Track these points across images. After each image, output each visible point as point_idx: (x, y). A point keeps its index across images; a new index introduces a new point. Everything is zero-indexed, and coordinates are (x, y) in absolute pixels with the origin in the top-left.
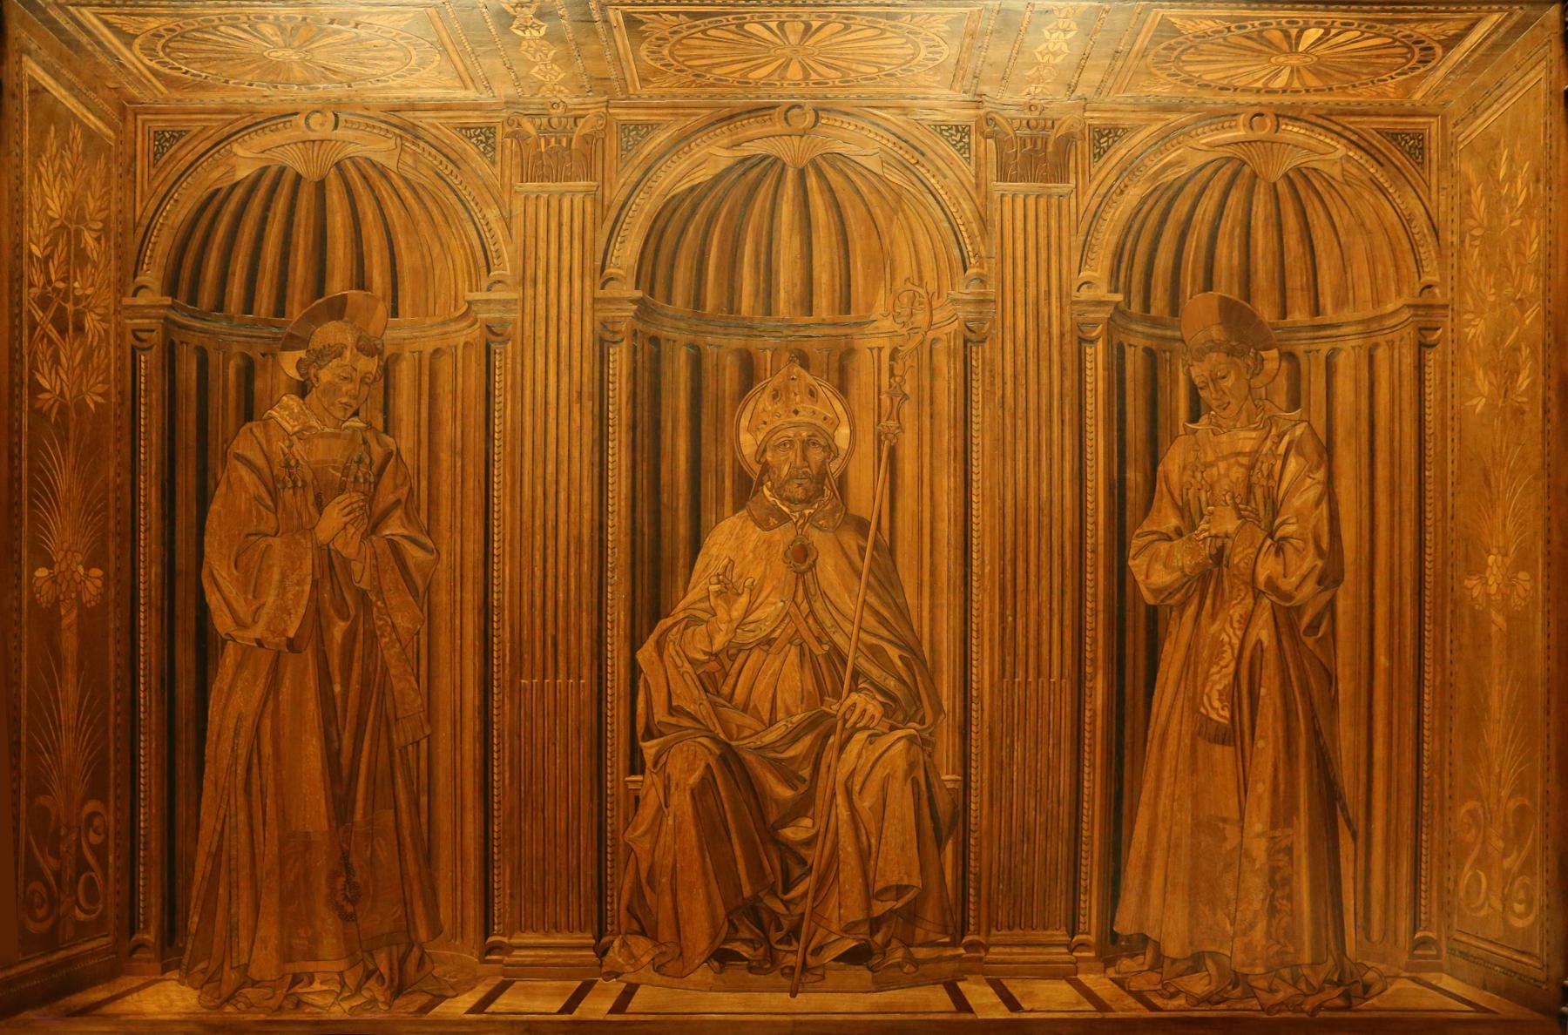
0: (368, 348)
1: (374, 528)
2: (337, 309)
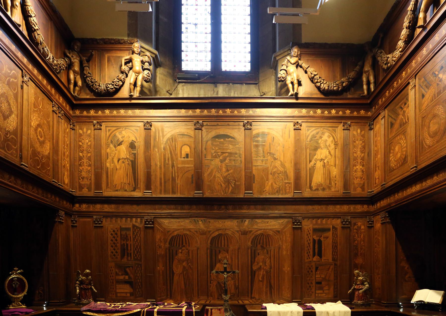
0: (187, 249)
1: (188, 264)
2: (184, 246)
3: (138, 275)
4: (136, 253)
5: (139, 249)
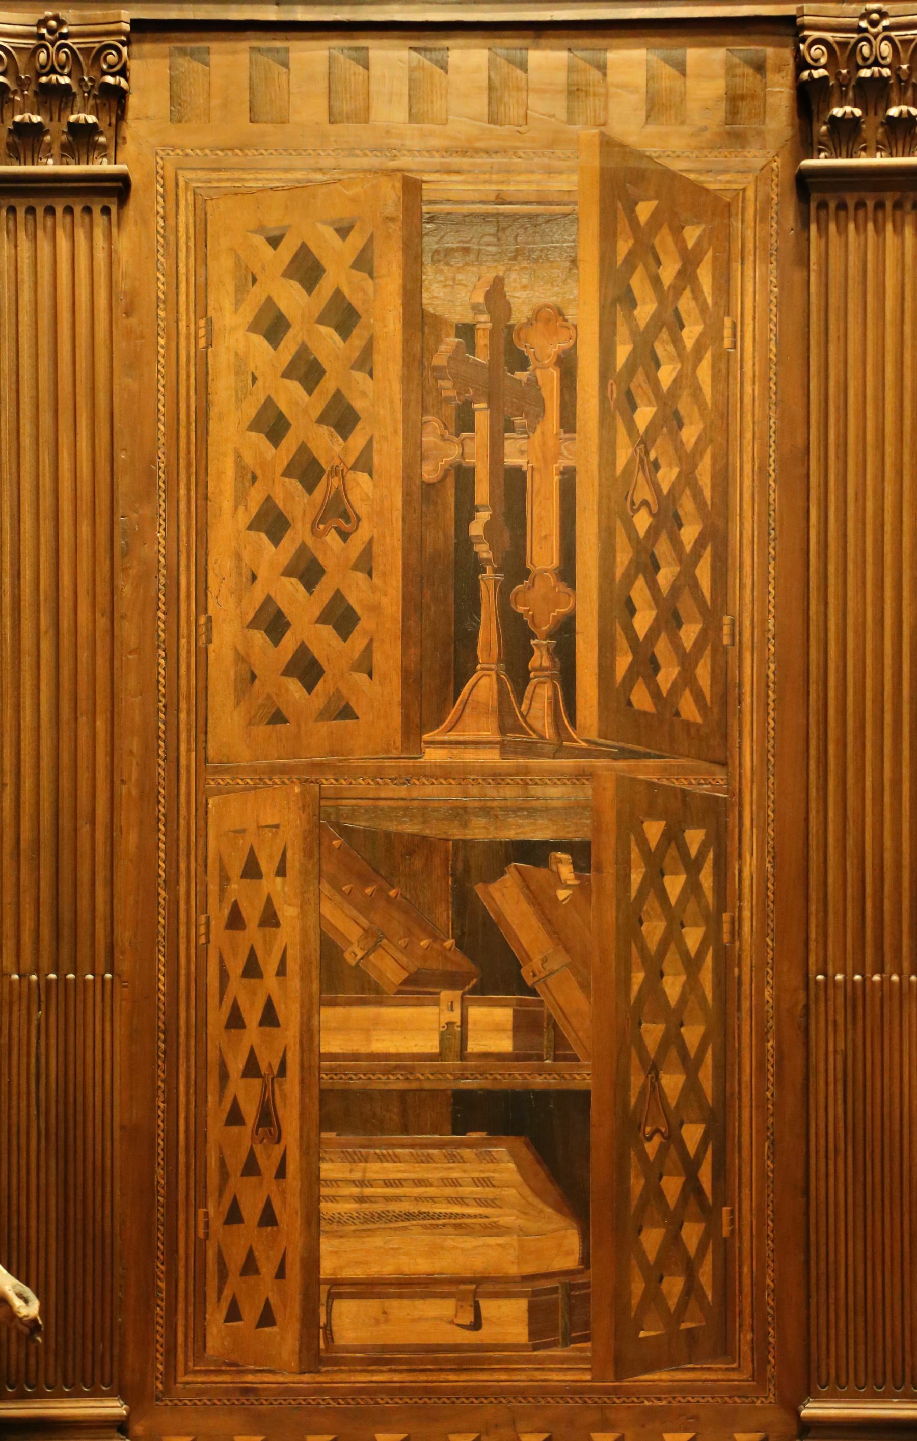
3: (673, 986)
4: (642, 622)
5: (688, 563)
